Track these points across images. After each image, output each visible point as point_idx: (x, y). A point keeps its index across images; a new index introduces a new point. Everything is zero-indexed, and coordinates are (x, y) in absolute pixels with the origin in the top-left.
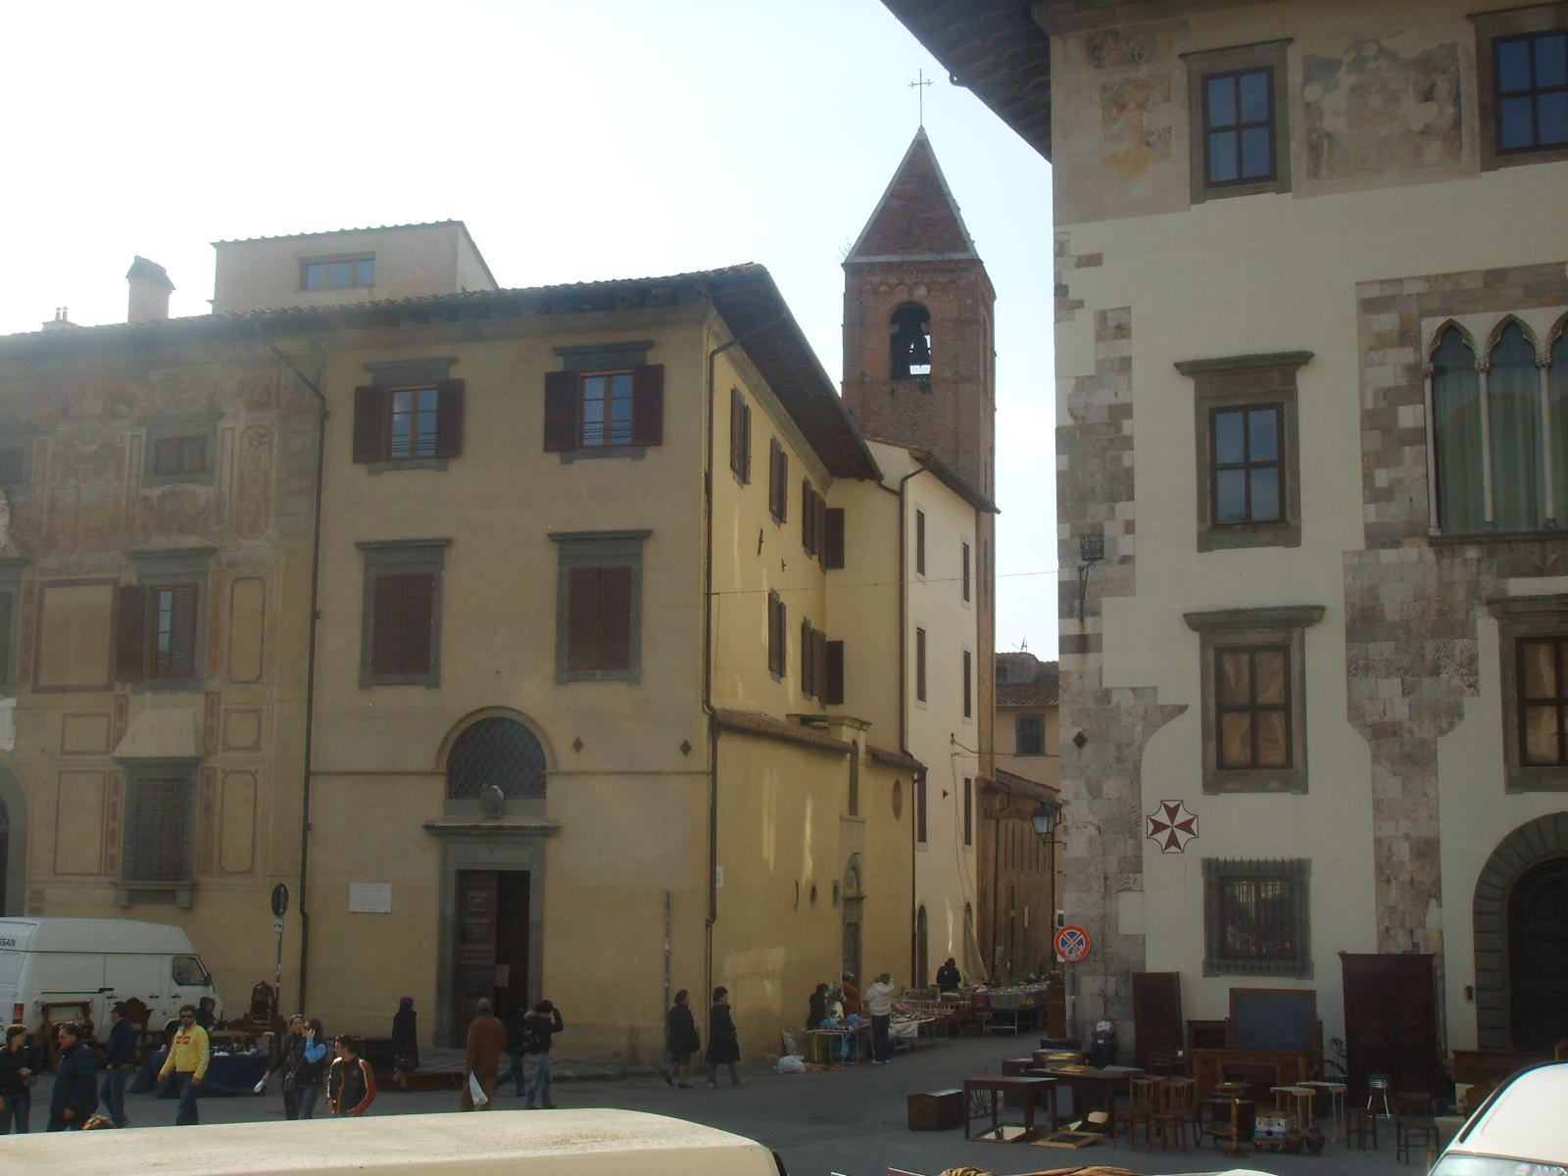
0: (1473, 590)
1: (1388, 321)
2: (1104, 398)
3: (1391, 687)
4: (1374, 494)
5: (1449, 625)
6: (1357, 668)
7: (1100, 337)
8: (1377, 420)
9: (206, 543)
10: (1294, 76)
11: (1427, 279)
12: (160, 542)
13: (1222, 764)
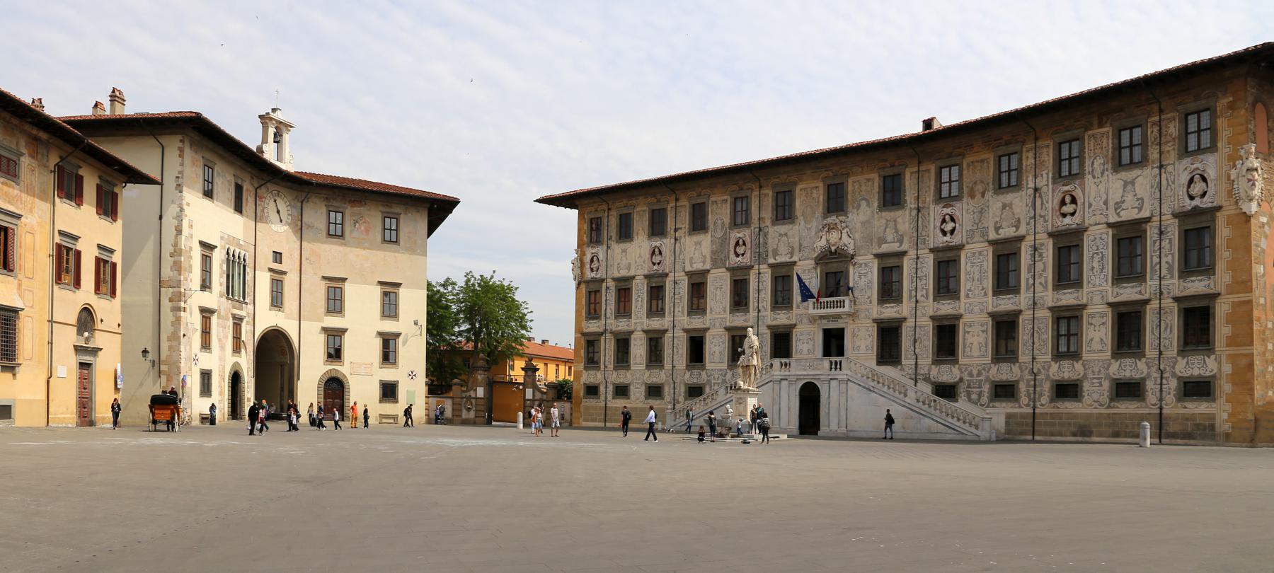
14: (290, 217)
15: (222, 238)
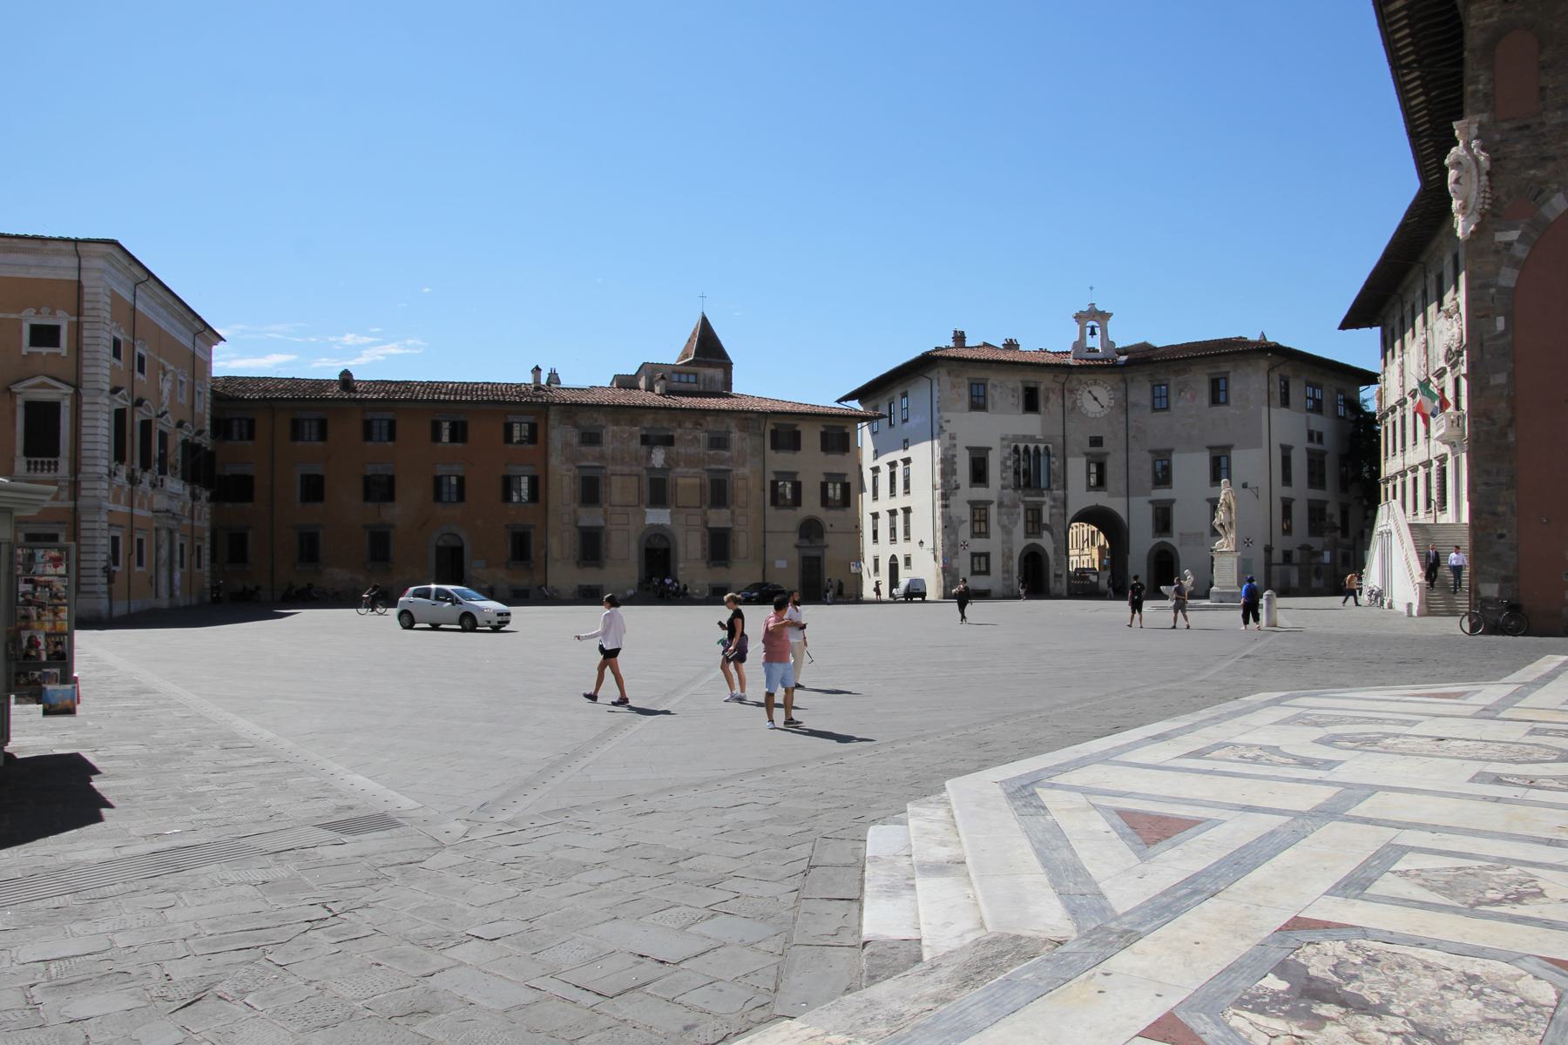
0: (1020, 498)
1: (1005, 443)
2: (950, 453)
3: (1005, 517)
4: (1003, 479)
5: (1016, 506)
6: (999, 514)
7: (950, 438)
8: (1003, 463)
9: (729, 468)
10: (989, 387)
11: (1014, 435)
12: (713, 466)
13: (974, 533)
14: (1113, 401)
15: (1003, 439)
